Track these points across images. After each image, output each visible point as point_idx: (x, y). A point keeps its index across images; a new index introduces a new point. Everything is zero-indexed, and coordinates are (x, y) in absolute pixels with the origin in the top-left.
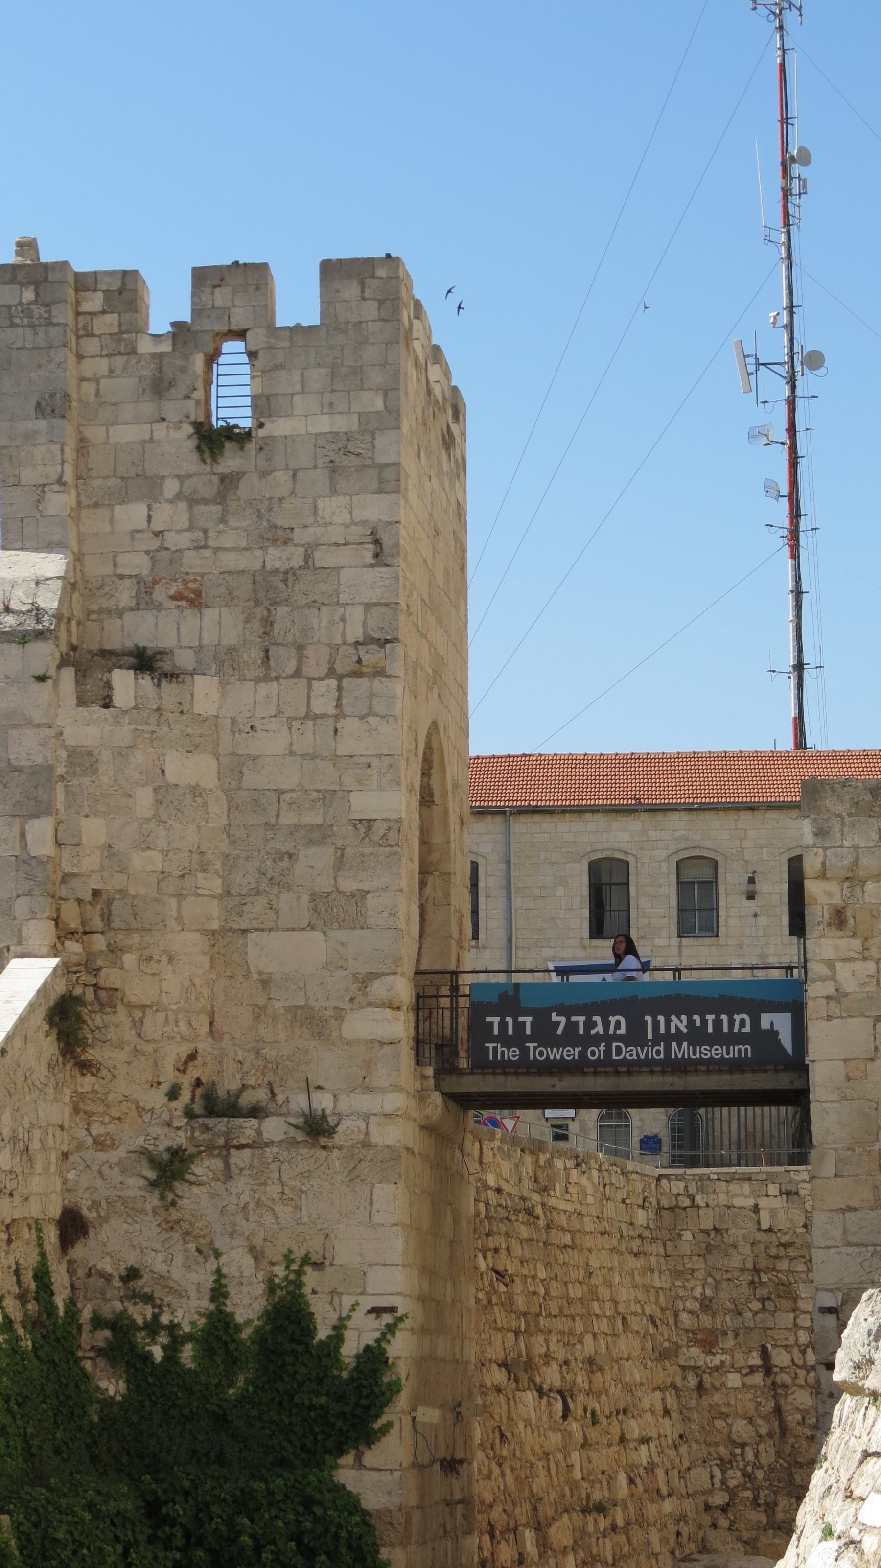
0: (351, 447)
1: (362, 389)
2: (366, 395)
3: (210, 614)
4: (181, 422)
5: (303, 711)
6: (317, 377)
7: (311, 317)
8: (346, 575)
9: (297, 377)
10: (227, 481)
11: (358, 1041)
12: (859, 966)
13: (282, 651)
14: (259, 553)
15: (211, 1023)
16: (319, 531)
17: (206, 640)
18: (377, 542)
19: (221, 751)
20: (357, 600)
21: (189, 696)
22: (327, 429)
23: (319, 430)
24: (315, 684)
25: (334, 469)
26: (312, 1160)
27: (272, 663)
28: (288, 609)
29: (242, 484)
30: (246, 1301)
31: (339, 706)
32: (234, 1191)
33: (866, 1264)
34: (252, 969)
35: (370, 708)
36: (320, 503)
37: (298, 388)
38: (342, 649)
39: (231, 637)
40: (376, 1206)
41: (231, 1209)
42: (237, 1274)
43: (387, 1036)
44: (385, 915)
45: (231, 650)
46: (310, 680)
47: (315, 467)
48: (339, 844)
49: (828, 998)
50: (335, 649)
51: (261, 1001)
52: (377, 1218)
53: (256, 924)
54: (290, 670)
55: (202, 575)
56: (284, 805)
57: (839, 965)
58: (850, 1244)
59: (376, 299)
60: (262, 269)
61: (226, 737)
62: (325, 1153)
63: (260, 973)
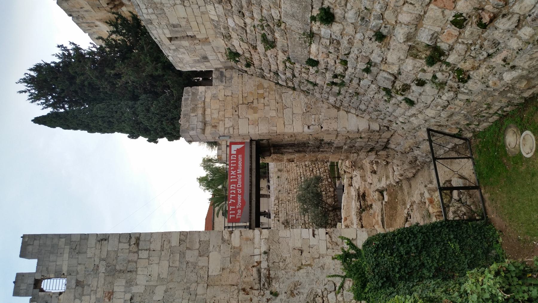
0: (74, 248)
1: (58, 245)
2: (60, 243)
3: (116, 289)
4: (58, 299)
5: (147, 260)
6: (52, 258)
7: (35, 261)
8: (110, 249)
9: (51, 264)
10: (78, 284)
11: (240, 242)
12: (226, 122)
13: (129, 267)
14: (100, 274)
15: (234, 285)
16: (96, 257)
17: (123, 290)
18: (102, 240)
19: (156, 284)
20: (117, 245)
21: (138, 294)
22: (68, 254)
23: (68, 257)
24: (139, 257)
25: (79, 253)
26: (273, 254)
27: (132, 270)
28: (117, 265)
29: (79, 280)
30: (313, 271)
31: (147, 250)
32: (282, 276)
33: (297, 120)
34: (219, 273)
35: (148, 241)
36: (88, 256)
37: (54, 263)
38: (131, 249)
39: (123, 282)
40: (285, 236)
41: (287, 276)
42: (306, 274)
43: (239, 234)
44: (206, 235)
45: (127, 282)
46: (138, 258)
47: (78, 258)
48: (186, 249)
49: (234, 129)
50: (130, 252)
51: (228, 270)
52: (289, 236)
53: (206, 273)
54: (135, 264)
55: (104, 292)
56: (173, 265)
57: (226, 126)
58: (293, 123)
59: (34, 241)
60: (18, 275)
61: (152, 283)
62: (271, 250)
63: (220, 271)
